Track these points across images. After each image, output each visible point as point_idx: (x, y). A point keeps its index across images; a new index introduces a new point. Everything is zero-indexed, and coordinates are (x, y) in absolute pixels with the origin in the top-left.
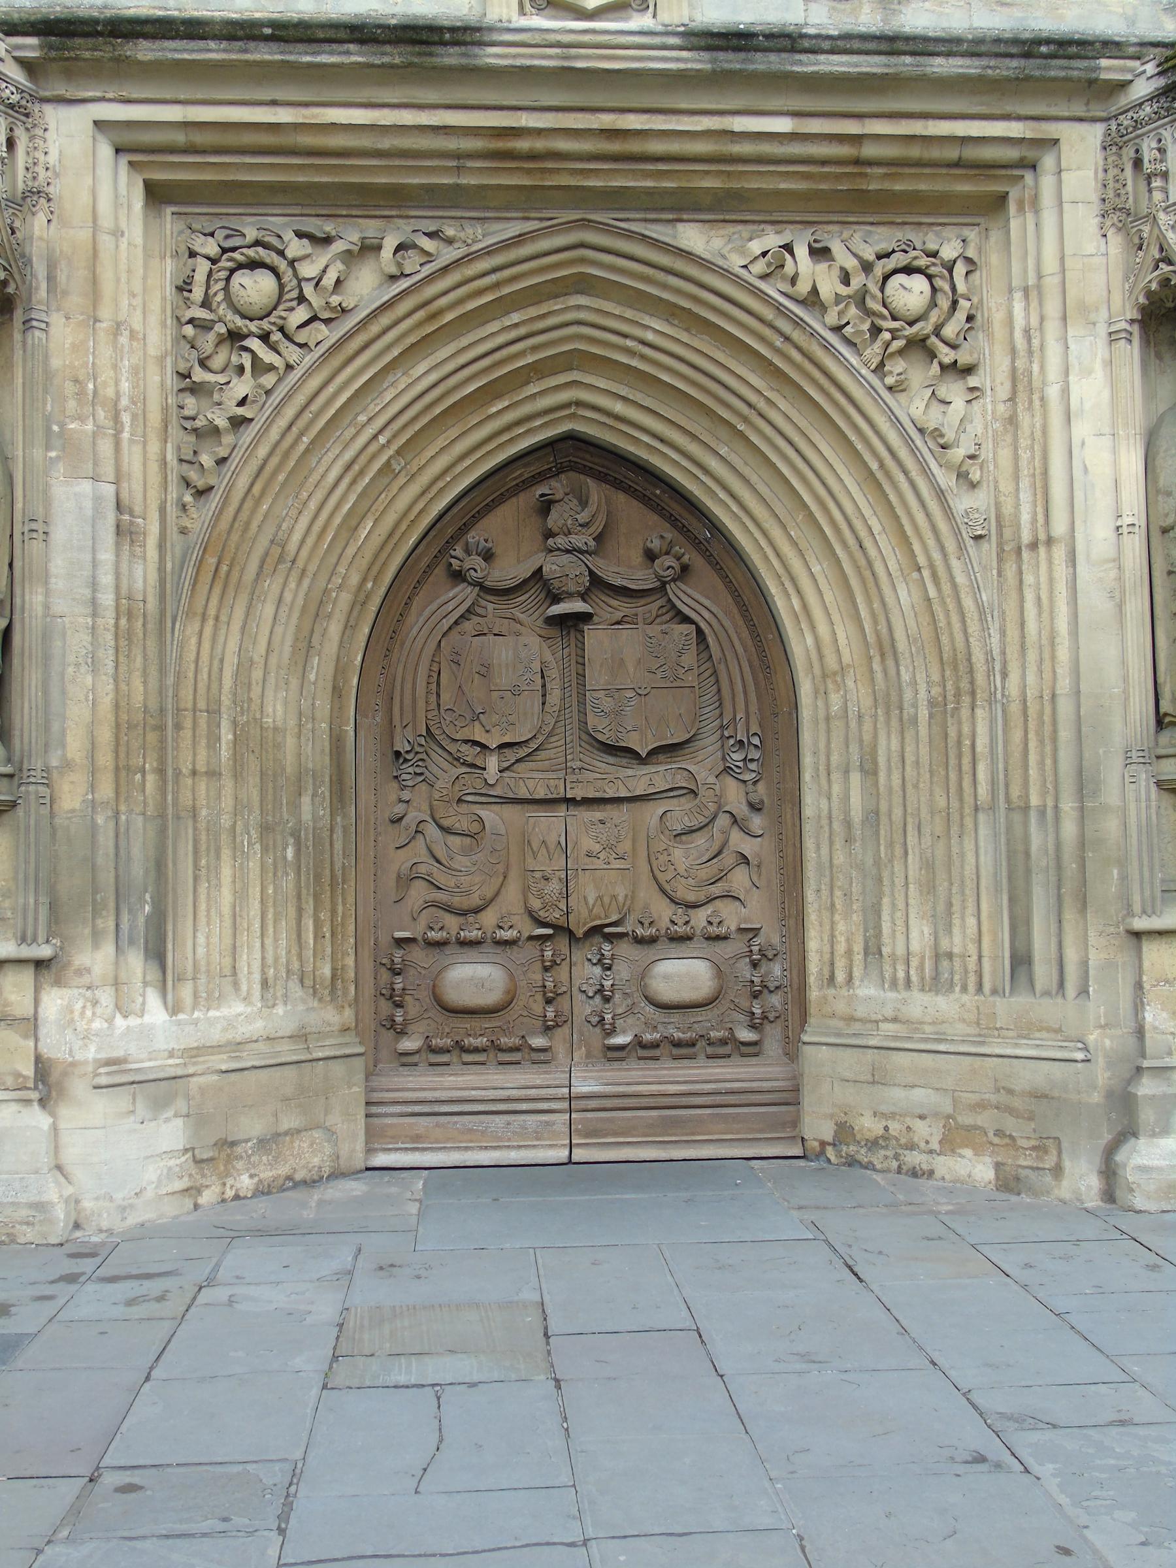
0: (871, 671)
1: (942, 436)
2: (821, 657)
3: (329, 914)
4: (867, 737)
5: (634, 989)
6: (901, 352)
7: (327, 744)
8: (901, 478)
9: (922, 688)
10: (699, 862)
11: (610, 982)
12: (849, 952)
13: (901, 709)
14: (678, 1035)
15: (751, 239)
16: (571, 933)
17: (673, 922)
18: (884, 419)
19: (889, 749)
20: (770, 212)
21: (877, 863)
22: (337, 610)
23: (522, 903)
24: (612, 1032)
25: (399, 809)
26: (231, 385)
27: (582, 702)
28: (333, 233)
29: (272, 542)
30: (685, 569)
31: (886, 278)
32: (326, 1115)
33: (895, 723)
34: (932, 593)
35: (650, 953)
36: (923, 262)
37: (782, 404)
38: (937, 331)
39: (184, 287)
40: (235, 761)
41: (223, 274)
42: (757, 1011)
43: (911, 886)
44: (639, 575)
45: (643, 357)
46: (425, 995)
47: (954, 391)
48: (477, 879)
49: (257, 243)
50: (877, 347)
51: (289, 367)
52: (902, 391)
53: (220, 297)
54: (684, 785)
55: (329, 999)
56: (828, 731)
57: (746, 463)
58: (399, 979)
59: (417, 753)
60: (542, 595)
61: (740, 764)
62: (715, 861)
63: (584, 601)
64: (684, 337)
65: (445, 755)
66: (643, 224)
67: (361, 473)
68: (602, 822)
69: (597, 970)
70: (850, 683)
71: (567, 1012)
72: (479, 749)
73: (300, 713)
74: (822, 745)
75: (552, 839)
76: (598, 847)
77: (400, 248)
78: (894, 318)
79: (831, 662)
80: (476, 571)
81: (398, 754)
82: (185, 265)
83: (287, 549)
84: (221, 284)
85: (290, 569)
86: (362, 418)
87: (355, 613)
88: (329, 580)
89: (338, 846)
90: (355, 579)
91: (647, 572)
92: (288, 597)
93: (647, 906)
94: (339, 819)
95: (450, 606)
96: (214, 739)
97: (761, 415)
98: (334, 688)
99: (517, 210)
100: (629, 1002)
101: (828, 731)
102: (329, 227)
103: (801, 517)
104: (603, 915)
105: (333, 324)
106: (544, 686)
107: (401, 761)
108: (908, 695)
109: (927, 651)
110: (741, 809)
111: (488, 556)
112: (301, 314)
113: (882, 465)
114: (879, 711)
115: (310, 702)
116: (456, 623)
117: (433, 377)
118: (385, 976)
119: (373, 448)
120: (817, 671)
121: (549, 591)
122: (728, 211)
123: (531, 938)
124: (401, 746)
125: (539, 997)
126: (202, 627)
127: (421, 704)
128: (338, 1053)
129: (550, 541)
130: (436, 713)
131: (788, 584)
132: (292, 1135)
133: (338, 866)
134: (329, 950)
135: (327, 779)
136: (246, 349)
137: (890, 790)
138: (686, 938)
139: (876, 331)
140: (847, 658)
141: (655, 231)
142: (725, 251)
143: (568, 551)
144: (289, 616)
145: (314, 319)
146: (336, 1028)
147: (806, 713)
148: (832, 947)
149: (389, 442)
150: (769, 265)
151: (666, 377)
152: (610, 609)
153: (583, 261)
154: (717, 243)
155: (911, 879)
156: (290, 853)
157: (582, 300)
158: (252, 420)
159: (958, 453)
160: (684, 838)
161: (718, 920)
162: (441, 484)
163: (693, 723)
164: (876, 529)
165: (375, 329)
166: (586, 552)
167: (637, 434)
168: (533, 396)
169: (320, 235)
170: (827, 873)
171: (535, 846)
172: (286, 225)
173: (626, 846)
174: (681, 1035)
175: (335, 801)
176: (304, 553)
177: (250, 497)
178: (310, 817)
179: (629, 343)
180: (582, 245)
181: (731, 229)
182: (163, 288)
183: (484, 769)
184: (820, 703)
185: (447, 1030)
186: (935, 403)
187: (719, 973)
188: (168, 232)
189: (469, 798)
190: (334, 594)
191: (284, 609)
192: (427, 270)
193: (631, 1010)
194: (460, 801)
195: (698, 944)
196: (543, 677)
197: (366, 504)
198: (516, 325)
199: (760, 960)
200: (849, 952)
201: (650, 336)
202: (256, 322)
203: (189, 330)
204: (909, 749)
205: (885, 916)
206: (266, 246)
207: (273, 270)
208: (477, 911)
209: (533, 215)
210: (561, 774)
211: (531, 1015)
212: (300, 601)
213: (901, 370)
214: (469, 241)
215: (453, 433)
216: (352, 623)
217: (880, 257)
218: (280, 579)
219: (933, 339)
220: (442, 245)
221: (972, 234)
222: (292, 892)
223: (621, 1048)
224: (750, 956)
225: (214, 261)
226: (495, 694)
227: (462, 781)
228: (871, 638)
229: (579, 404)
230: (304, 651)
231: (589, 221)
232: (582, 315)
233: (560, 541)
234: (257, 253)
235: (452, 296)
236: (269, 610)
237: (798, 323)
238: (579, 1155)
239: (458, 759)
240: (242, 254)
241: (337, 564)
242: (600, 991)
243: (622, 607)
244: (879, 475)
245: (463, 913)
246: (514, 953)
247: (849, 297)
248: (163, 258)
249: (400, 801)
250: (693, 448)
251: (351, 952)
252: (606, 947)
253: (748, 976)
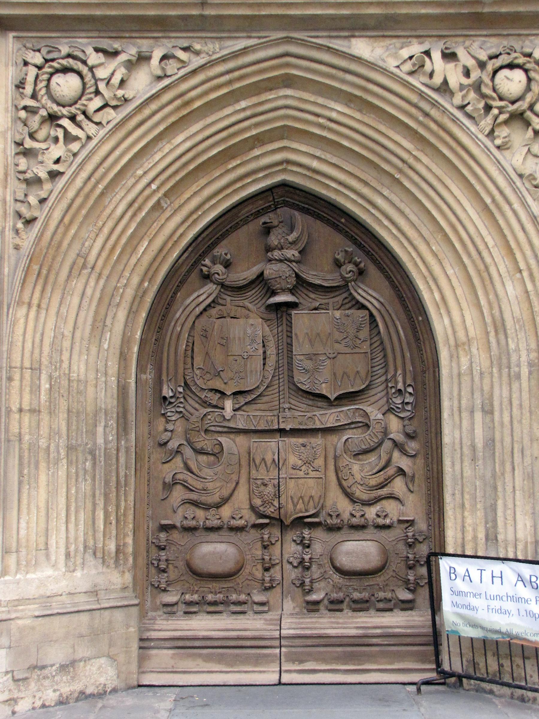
0: (489, 342)
1: (535, 179)
2: (454, 332)
3: (114, 508)
4: (486, 388)
5: (326, 562)
6: (506, 122)
7: (115, 391)
8: (506, 208)
9: (524, 353)
10: (370, 473)
11: (309, 556)
12: (475, 538)
13: (509, 367)
14: (356, 595)
15: (402, 48)
16: (282, 521)
17: (353, 516)
18: (494, 168)
19: (501, 396)
20: (415, 30)
21: (494, 476)
22: (124, 301)
23: (248, 502)
24: (310, 591)
25: (166, 436)
26: (50, 150)
27: (290, 364)
28: (120, 49)
29: (78, 255)
30: (361, 272)
31: (495, 72)
32: (110, 648)
33: (505, 378)
34: (530, 287)
35: (337, 537)
36: (521, 60)
37: (425, 159)
38: (531, 108)
39: (20, 85)
40: (50, 402)
41: (46, 77)
42: (411, 578)
43: (517, 493)
44: (329, 277)
45: (330, 130)
46: (181, 564)
48: (218, 484)
49: (69, 56)
50: (489, 119)
51: (89, 138)
52: (508, 149)
53: (43, 91)
54: (360, 420)
55: (114, 566)
56: (460, 384)
57: (402, 201)
58: (163, 553)
59: (178, 398)
60: (264, 291)
61: (400, 406)
62: (382, 473)
63: (293, 294)
64: (358, 115)
65: (197, 399)
66: (328, 40)
67: (140, 209)
68: (304, 446)
69: (300, 548)
70: (474, 351)
71: (278, 577)
72: (220, 395)
73: (97, 371)
74: (455, 393)
75: (269, 458)
76: (300, 463)
77: (164, 58)
78: (501, 99)
79: (461, 335)
80: (218, 274)
81: (165, 398)
82: (21, 70)
83: (88, 259)
84: (44, 84)
85: (90, 273)
86: (140, 172)
87: (136, 303)
88: (118, 281)
89: (122, 460)
90: (135, 280)
91: (335, 275)
92: (89, 291)
93: (335, 504)
94: (123, 442)
95: (201, 299)
96: (35, 389)
97: (411, 168)
98: (121, 353)
99: (243, 30)
100: (322, 570)
101: (460, 384)
102: (117, 45)
103: (439, 237)
104: (304, 510)
105: (119, 109)
106: (264, 352)
107: (167, 403)
108: (514, 358)
109: (527, 328)
110: (400, 438)
111: (227, 265)
112: (97, 103)
113: (494, 200)
114: (494, 369)
115: (104, 363)
116: (205, 310)
117: (188, 144)
118: (154, 550)
119: (147, 192)
120: (452, 342)
121: (269, 288)
122: (386, 29)
123: (254, 526)
124: (167, 392)
125: (260, 567)
126: (28, 311)
127: (181, 365)
128: (119, 604)
129: (269, 254)
130: (190, 371)
131: (431, 283)
132: (85, 661)
133: (122, 474)
134: (114, 532)
135: (115, 415)
136: (60, 126)
137: (502, 424)
138: (362, 527)
139: (488, 108)
140: (472, 333)
141: (337, 44)
142: (384, 56)
143: (281, 261)
144: (90, 305)
145: (106, 105)
146: (119, 586)
147: (445, 371)
148: (463, 534)
149: (158, 188)
150: (414, 65)
151: (346, 143)
152: (310, 300)
153: (288, 65)
155: (517, 488)
156: (88, 464)
157: (289, 92)
158: (63, 173)
160: (360, 457)
161: (384, 514)
162: (195, 216)
163: (367, 377)
164: (491, 243)
165: (147, 112)
166: (294, 261)
167: (327, 182)
168: (257, 157)
169: (111, 50)
170: (460, 482)
171: (258, 462)
172: (89, 44)
173: (320, 462)
174: (358, 594)
175: (120, 430)
176: (100, 263)
177: (62, 224)
178: (102, 441)
179: (321, 120)
180: (287, 54)
181: (388, 42)
182: (6, 87)
183: (223, 409)
184: (454, 365)
185: (196, 589)
186: (530, 157)
187: (385, 552)
188: (11, 49)
189: (212, 428)
190: (121, 290)
191: (86, 300)
192: (182, 72)
193: (323, 577)
194: (206, 431)
195: (370, 533)
196: (264, 346)
197: (143, 230)
198: (244, 109)
199: (413, 543)
200: (475, 538)
201: (334, 115)
202: (67, 108)
203: (23, 114)
204: (515, 396)
205: (500, 513)
206: (75, 58)
207: (79, 74)
208: (218, 506)
209: (254, 35)
210: (275, 413)
211: (255, 579)
212: (98, 295)
213: (506, 135)
214: (211, 53)
215: (203, 182)
216: (134, 309)
217: (491, 58)
218: (83, 280)
219: (529, 114)
220: (192, 56)
222: (89, 492)
223: (317, 603)
224: (406, 540)
225: (40, 68)
226: (231, 358)
227: (209, 417)
228: (488, 320)
229: (288, 162)
230: (100, 328)
231: (292, 38)
232: (289, 102)
233: (276, 254)
234: (68, 62)
235: (199, 90)
236: (76, 300)
237: (435, 104)
238: (286, 678)
239: (205, 402)
240: (59, 63)
241: (124, 270)
242: (302, 561)
243: (317, 299)
244: (492, 207)
245: (207, 507)
246: (243, 536)
247: (469, 85)
248: (7, 66)
249: (166, 430)
250: (365, 191)
251: (131, 534)
252: (306, 533)
253: (405, 553)
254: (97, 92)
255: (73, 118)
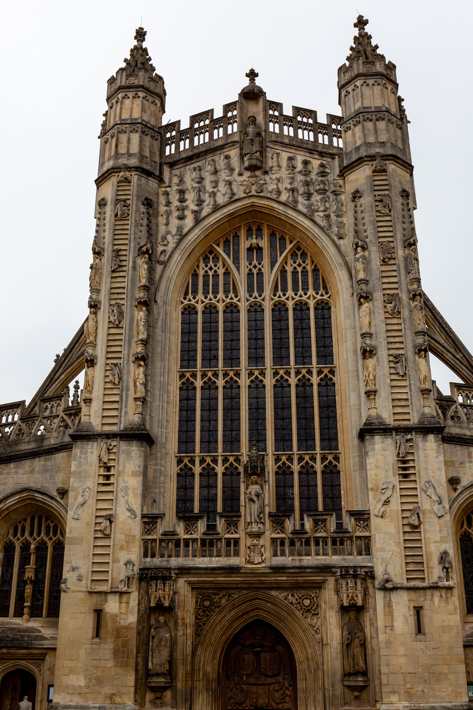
38: (311, 608)
39: (197, 602)
47: (315, 618)
154: (277, 593)
159: (315, 628)
221: (318, 591)
254: (214, 605)
255: (208, 611)
